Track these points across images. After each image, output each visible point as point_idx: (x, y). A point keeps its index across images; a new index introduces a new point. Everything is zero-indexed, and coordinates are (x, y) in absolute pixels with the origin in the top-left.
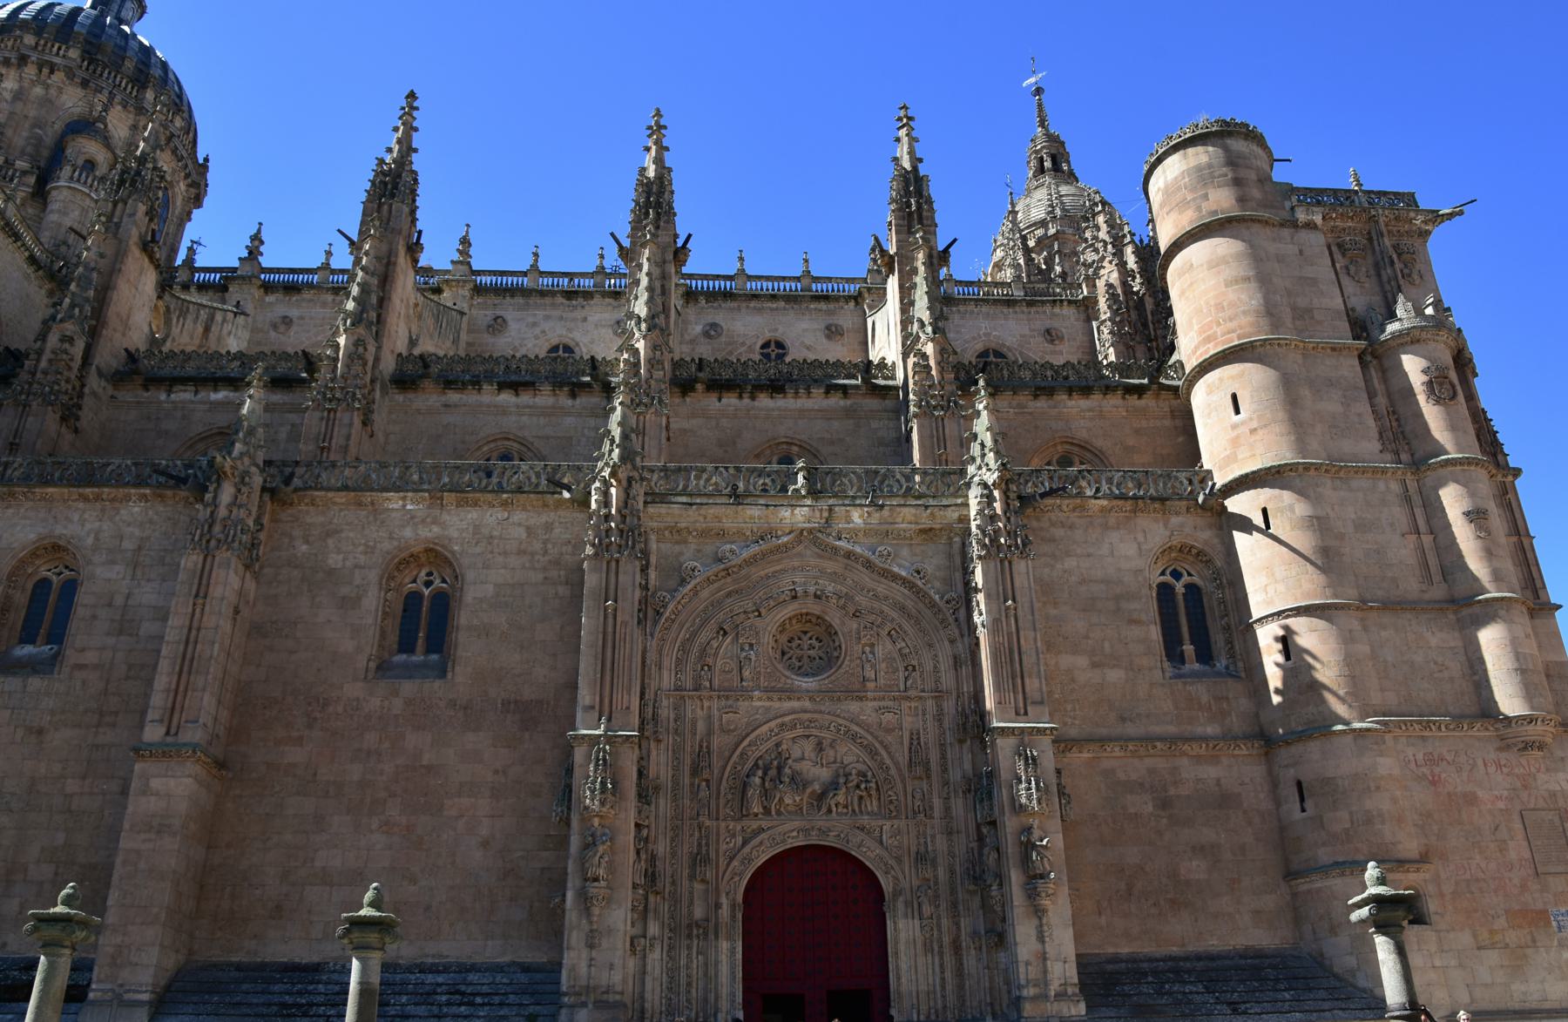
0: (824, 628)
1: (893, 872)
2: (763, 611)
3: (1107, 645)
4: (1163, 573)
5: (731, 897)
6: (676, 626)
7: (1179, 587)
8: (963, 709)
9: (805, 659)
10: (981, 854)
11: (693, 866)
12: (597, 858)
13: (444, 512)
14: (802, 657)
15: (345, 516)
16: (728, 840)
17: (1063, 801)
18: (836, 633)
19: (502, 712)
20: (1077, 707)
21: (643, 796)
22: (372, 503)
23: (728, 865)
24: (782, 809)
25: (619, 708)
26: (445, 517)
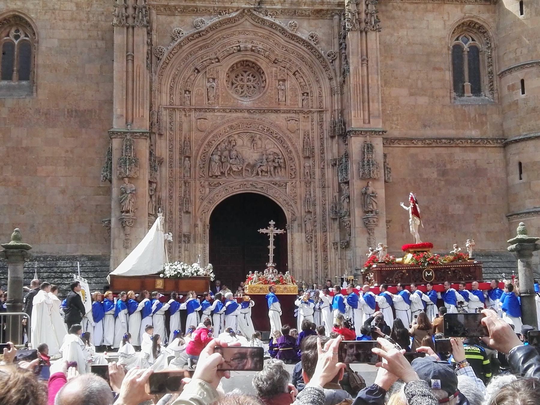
3: (419, 83)
4: (457, 39)
7: (466, 47)
9: (245, 88)
10: (340, 200)
12: (128, 201)
17: (386, 172)
18: (263, 73)
19: (68, 116)
20: (399, 118)
21: (153, 168)
23: (201, 203)
25: (137, 116)
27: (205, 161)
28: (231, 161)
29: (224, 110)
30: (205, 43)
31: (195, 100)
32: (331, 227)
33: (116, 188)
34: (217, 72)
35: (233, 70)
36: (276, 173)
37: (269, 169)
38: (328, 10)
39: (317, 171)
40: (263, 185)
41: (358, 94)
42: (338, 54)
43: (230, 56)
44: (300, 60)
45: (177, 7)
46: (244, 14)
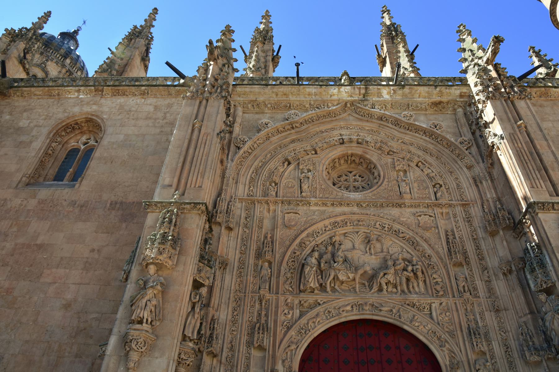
0: (365, 166)
1: (447, 346)
2: (318, 150)
5: (287, 364)
6: (252, 156)
8: (490, 211)
11: (251, 334)
12: (144, 301)
13: (103, 99)
14: (349, 187)
15: (40, 102)
16: (286, 311)
18: (375, 167)
22: (58, 95)
24: (336, 287)
25: (193, 186)
26: (103, 101)
27: (294, 269)
31: (283, 193)
33: (133, 285)
37: (398, 281)
41: (528, 161)
46: (346, 109)
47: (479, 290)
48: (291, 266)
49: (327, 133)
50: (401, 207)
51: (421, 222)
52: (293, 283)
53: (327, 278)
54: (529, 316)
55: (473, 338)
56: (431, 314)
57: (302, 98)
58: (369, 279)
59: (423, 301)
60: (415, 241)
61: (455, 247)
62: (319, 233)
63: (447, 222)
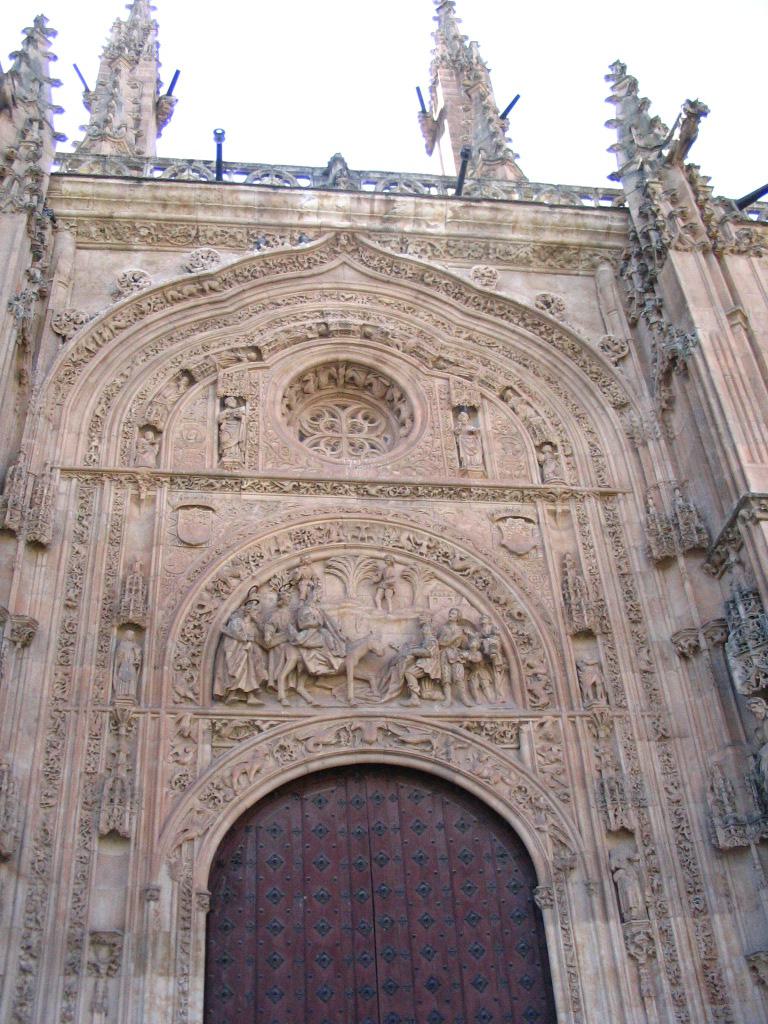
9: (344, 446)
18: (403, 397)
28: (301, 637)
29: (276, 484)
30: (218, 312)
32: (721, 889)
34: (255, 385)
35: (304, 392)
36: (477, 693)
37: (447, 675)
38: (580, 247)
39: (630, 680)
40: (430, 730)
41: (746, 401)
42: (631, 344)
43: (296, 347)
44: (517, 364)
45: (137, 225)
47: (627, 692)
48: (193, 640)
49: (288, 308)
50: (458, 494)
51: (505, 533)
52: (196, 679)
53: (280, 666)
54: (730, 751)
55: (609, 801)
56: (518, 748)
57: (227, 216)
58: (381, 670)
59: (503, 720)
60: (489, 579)
61: (579, 594)
62: (262, 557)
63: (564, 534)
